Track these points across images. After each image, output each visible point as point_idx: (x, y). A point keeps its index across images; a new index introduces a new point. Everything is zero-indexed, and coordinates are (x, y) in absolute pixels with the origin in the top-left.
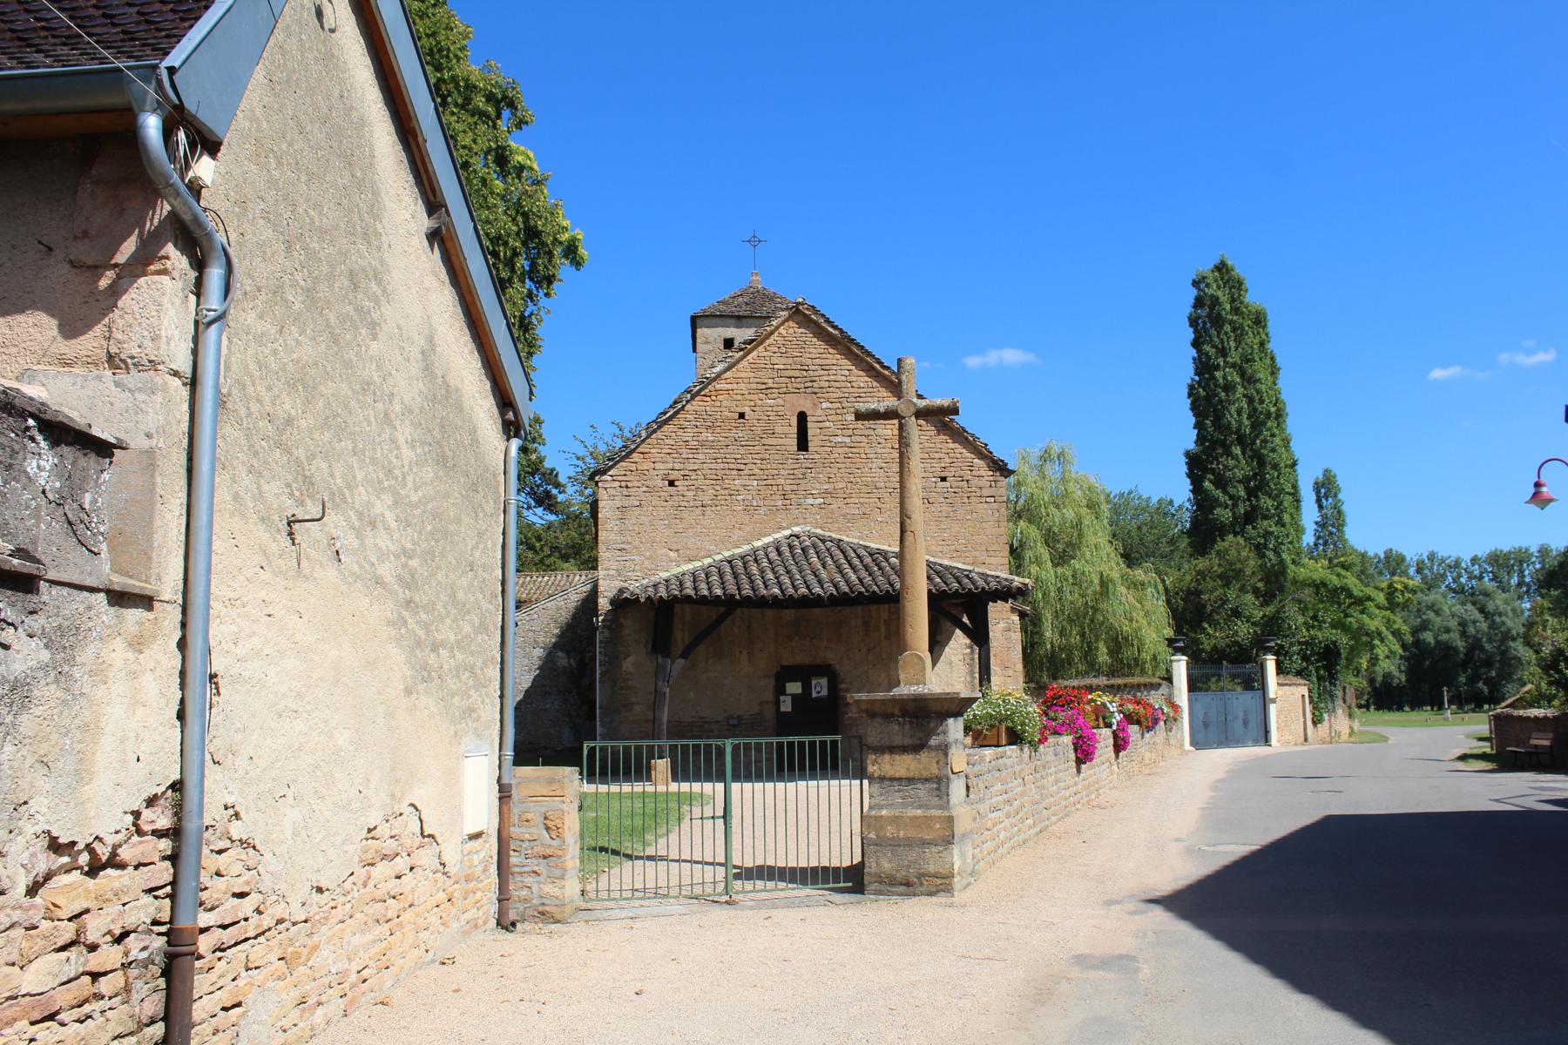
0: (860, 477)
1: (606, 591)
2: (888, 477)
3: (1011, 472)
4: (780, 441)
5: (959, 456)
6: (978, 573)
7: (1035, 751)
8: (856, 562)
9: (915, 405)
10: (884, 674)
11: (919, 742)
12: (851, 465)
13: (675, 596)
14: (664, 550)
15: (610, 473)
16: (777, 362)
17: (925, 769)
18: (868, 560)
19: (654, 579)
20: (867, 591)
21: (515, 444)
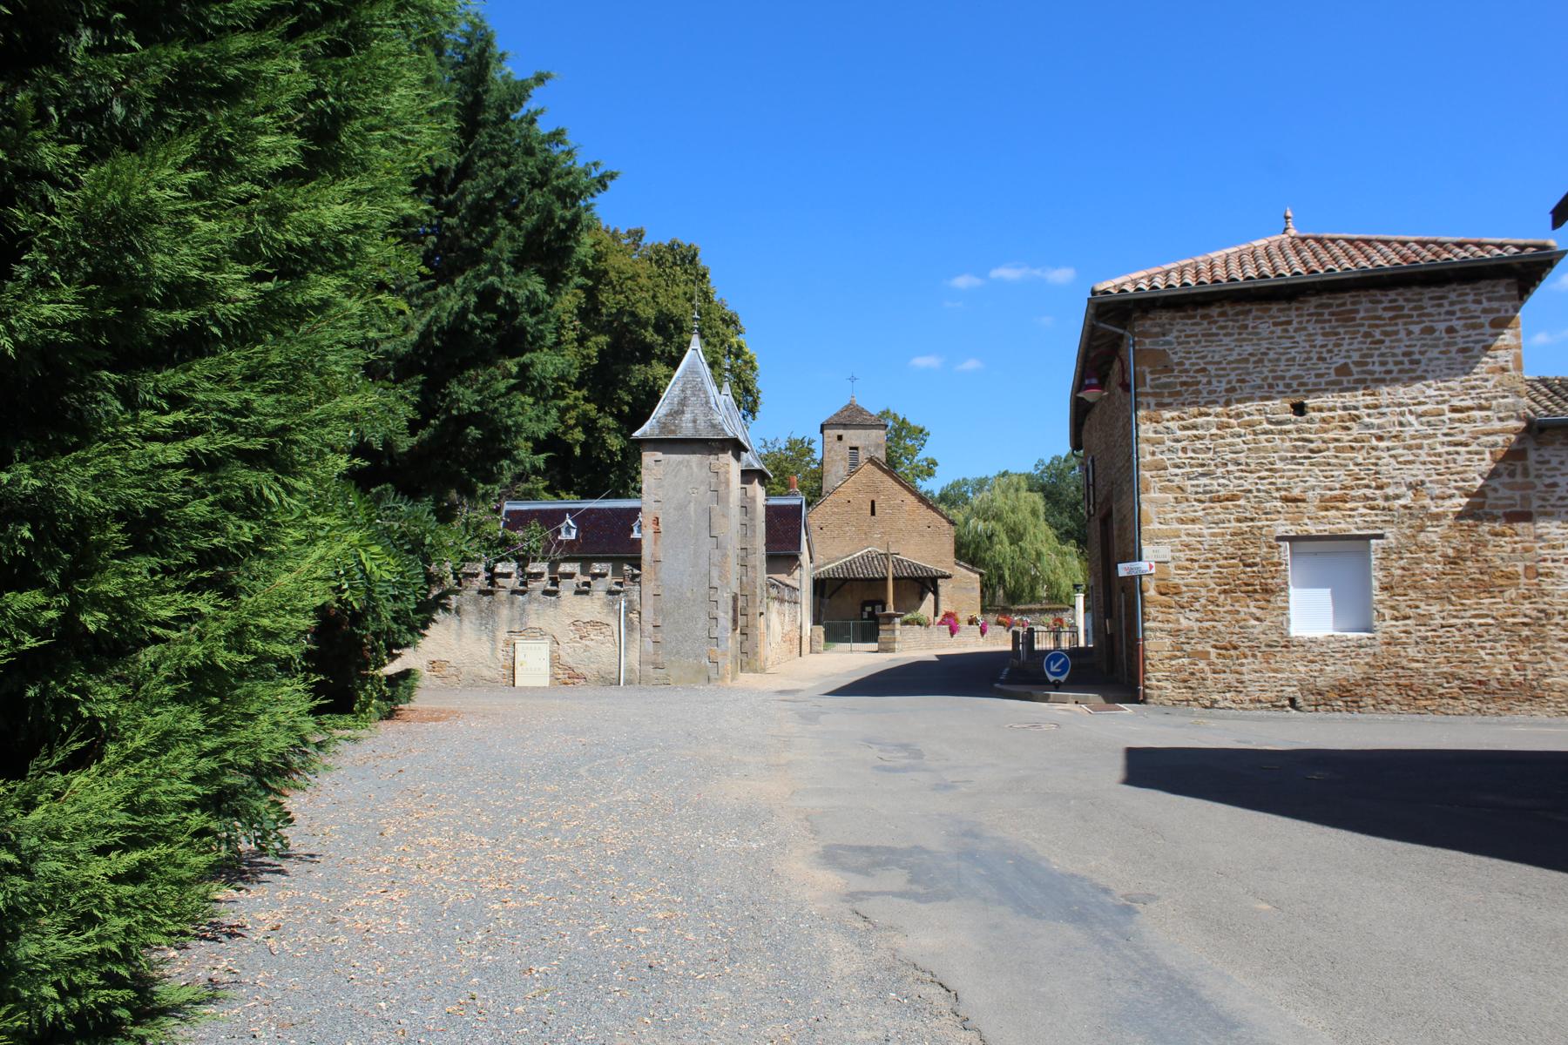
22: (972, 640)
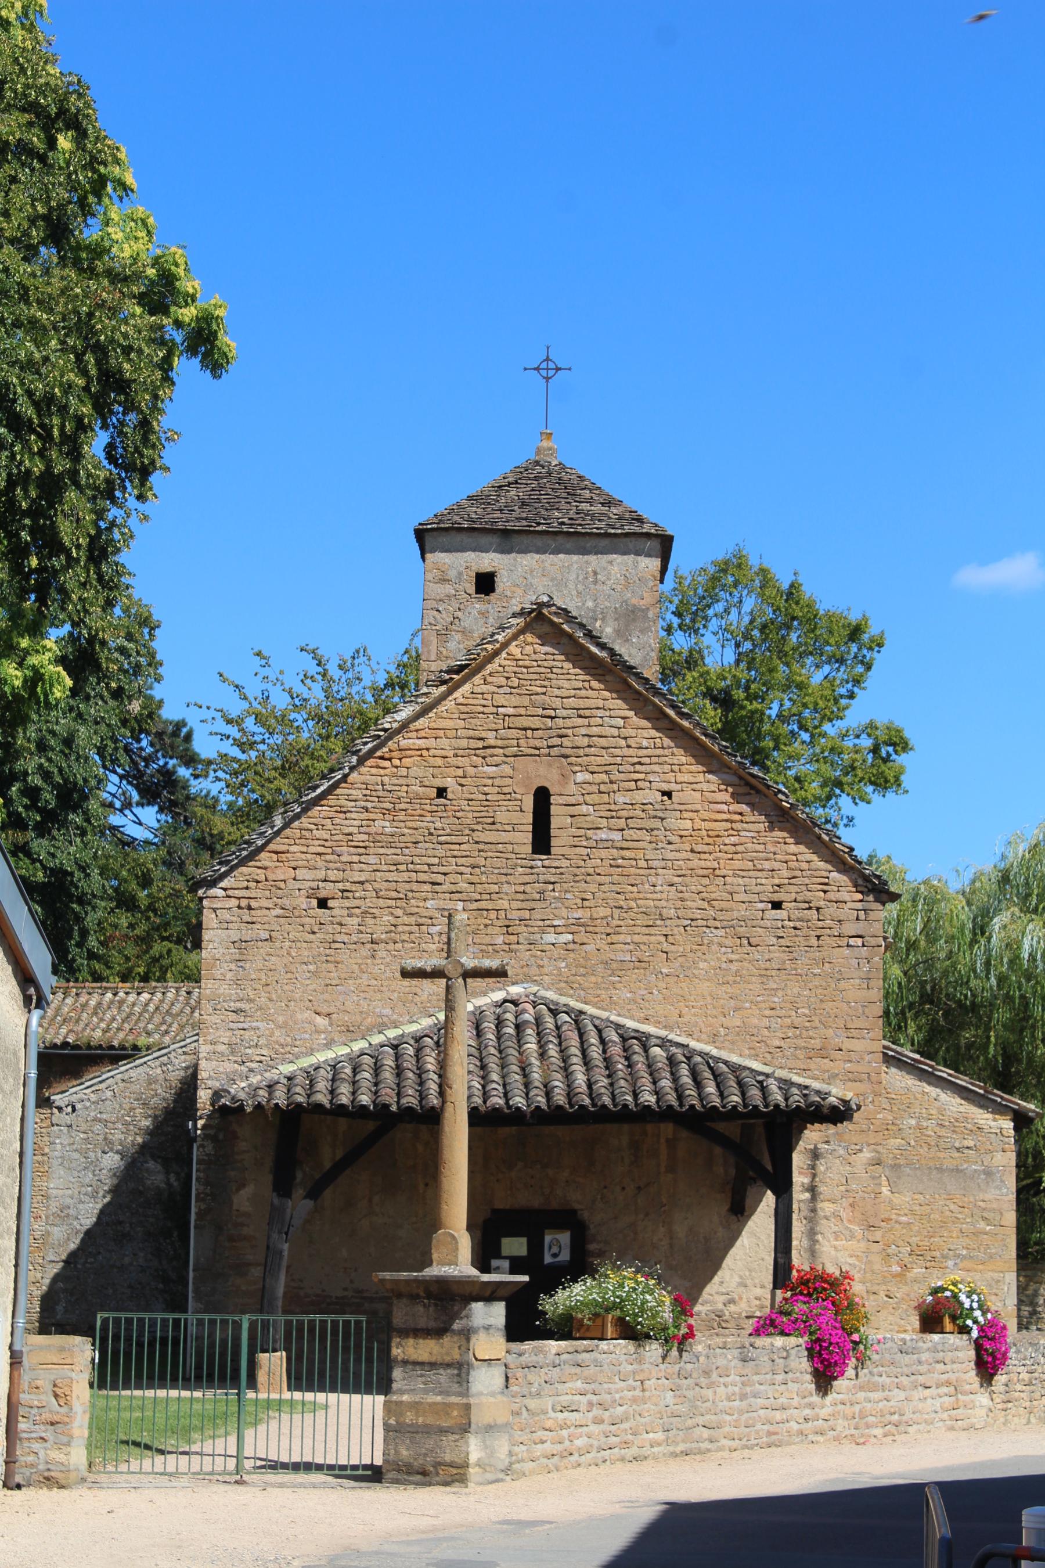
0: (635, 900)
1: (210, 1078)
2: (682, 900)
3: (894, 897)
4: (504, 837)
5: (805, 866)
6: (780, 1080)
7: (680, 1351)
8: (595, 1053)
9: (462, 965)
10: (662, 1229)
11: (442, 1325)
12: (621, 879)
13: (299, 1105)
14: (307, 1014)
15: (222, 885)
16: (500, 700)
17: (447, 1354)
18: (615, 1050)
19: (272, 1075)
20: (594, 1105)
21: (36, 1014)
22: (934, 1401)
